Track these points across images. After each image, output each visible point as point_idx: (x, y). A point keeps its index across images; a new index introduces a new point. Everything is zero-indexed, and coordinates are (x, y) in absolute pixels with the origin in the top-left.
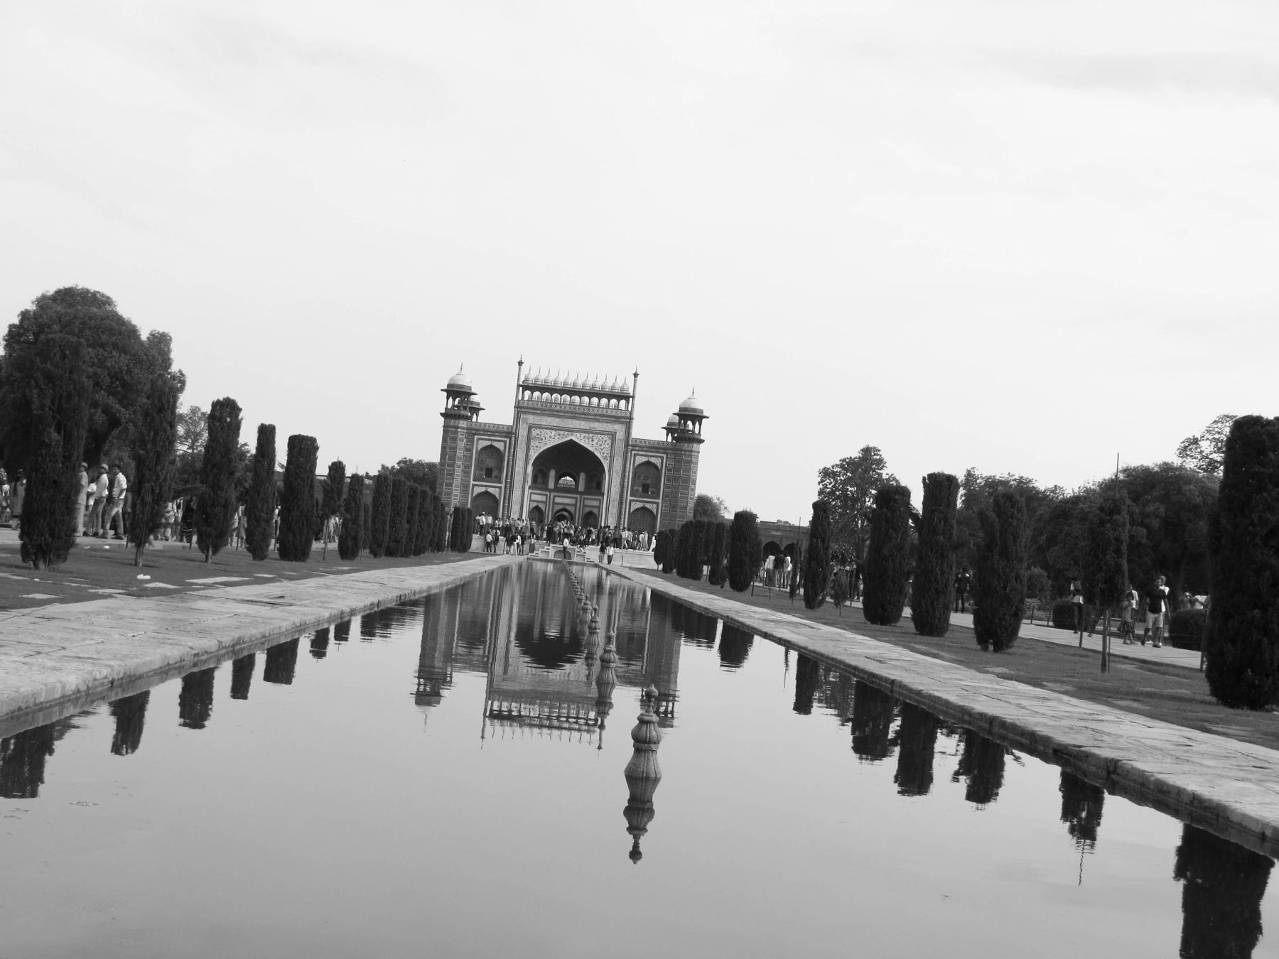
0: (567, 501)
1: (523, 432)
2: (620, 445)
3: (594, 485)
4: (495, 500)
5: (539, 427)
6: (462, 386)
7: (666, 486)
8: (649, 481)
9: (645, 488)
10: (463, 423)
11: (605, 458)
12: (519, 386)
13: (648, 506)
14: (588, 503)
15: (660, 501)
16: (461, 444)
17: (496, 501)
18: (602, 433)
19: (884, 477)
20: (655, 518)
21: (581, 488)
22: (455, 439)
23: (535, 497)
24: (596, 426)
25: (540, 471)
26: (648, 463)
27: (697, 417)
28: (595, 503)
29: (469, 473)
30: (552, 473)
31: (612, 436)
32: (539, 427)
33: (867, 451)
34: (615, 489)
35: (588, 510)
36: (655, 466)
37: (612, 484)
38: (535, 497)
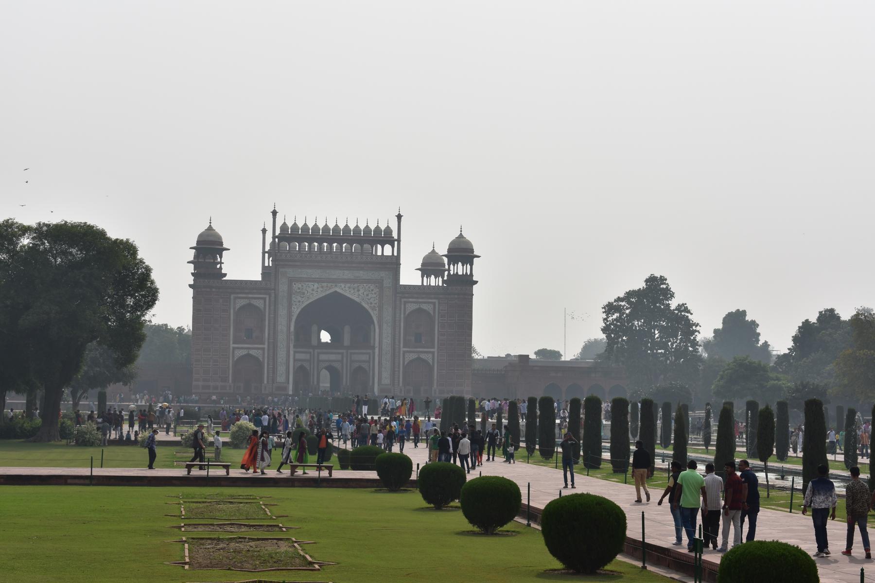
1: (283, 288)
5: (300, 280)
11: (373, 309)
13: (423, 356)
15: (435, 350)
17: (258, 363)
18: (368, 281)
19: (673, 307)
21: (347, 342)
23: (299, 356)
24: (362, 274)
26: (420, 310)
28: (364, 357)
30: (315, 328)
34: (387, 341)
37: (383, 335)
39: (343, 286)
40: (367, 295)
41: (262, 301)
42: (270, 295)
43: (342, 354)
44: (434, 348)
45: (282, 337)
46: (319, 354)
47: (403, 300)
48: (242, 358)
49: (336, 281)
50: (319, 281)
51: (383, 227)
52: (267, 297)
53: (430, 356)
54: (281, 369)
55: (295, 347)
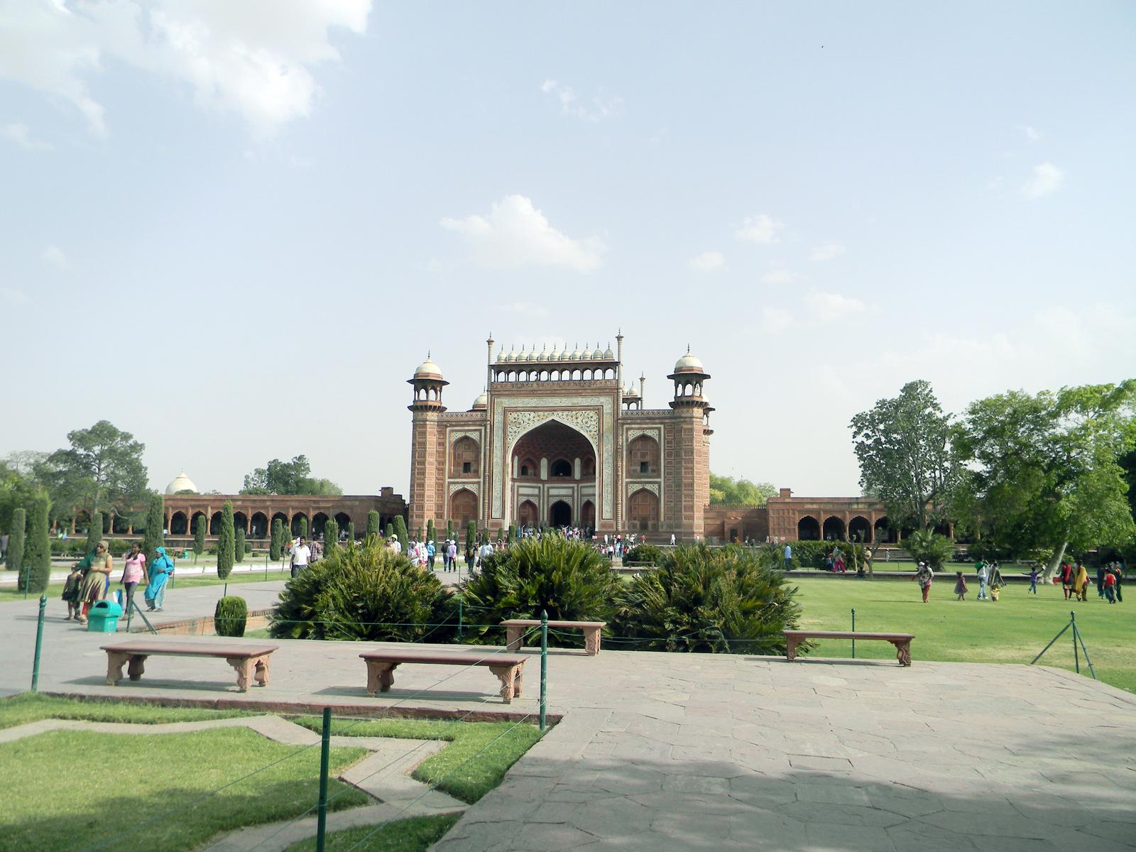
0: (563, 492)
1: (498, 418)
2: (608, 421)
3: (591, 471)
4: (474, 498)
5: (516, 410)
6: (428, 375)
7: (668, 463)
8: (648, 459)
9: (644, 465)
10: (432, 416)
12: (491, 367)
13: (648, 487)
14: (586, 491)
15: (662, 480)
16: (432, 439)
18: (586, 408)
20: (657, 500)
22: (424, 433)
23: (522, 491)
25: (528, 460)
26: (644, 438)
27: (696, 378)
28: (589, 491)
29: (443, 470)
30: (544, 462)
31: (598, 410)
32: (516, 410)
33: (910, 389)
35: (585, 499)
36: (653, 440)
38: (522, 491)
39: (560, 413)
40: (586, 423)
41: (478, 433)
42: (485, 426)
43: (573, 488)
44: (659, 476)
45: (497, 470)
46: (549, 488)
47: (625, 426)
48: (457, 493)
49: (553, 410)
50: (535, 410)
51: (603, 350)
52: (483, 428)
53: (656, 486)
54: (496, 503)
55: (513, 480)
